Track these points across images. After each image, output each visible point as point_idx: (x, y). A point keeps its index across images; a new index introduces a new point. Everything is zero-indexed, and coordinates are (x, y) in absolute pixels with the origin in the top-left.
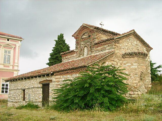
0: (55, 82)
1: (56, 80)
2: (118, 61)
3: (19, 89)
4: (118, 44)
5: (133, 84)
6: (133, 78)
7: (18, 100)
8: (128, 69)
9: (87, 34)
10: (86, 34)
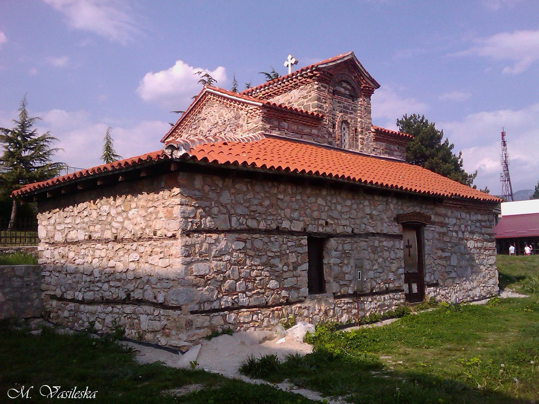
0: (434, 223)
1: (436, 220)
3: (291, 233)
7: (284, 293)
9: (348, 87)
10: (345, 85)
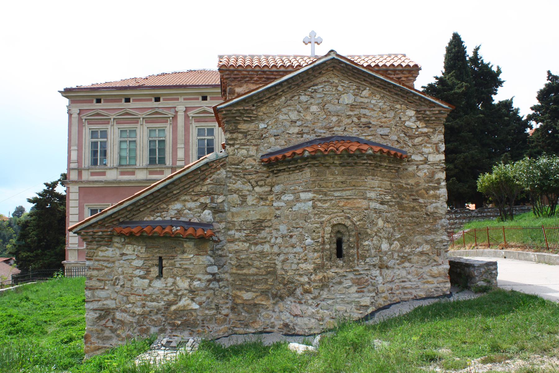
2: (250, 188)
4: (252, 121)
5: (301, 275)
6: (301, 250)
8: (287, 217)
